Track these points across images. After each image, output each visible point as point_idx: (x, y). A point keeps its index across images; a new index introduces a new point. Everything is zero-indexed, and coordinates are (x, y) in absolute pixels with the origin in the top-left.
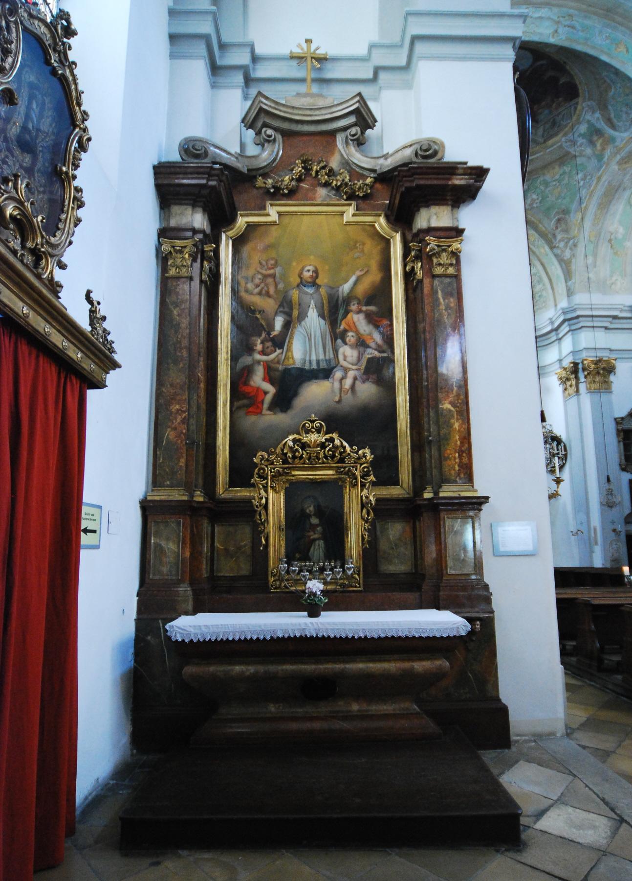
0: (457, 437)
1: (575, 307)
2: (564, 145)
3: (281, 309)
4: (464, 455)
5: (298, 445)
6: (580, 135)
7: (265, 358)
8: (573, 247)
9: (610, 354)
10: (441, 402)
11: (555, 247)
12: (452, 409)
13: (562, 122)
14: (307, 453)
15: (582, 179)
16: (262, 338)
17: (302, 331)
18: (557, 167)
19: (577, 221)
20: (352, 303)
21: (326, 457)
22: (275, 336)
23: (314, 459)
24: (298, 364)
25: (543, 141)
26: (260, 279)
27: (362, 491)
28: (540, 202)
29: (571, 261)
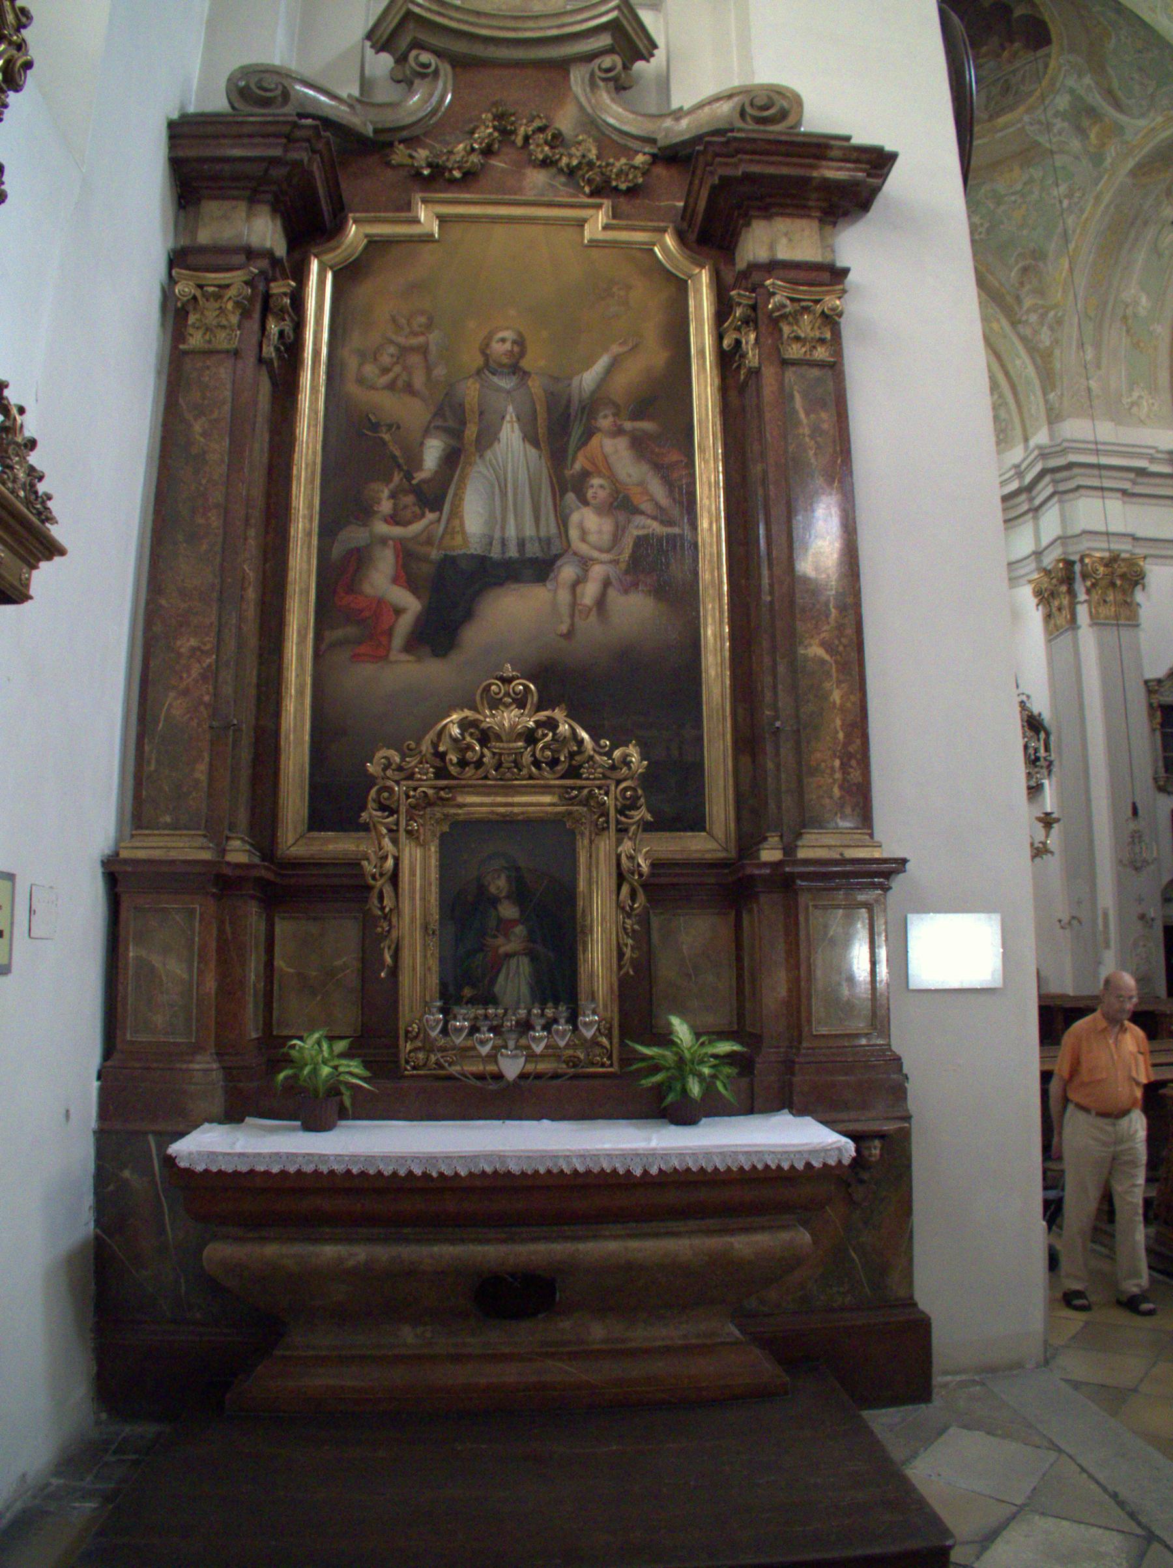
0: (838, 722)
1: (1065, 444)
2: (1027, 127)
3: (439, 423)
4: (853, 763)
5: (471, 735)
6: (1057, 114)
7: (397, 531)
9: (1133, 546)
10: (801, 643)
11: (1020, 322)
12: (827, 657)
13: (1022, 88)
14: (494, 754)
15: (1065, 197)
16: (392, 486)
17: (485, 472)
18: (1017, 169)
20: (602, 414)
21: (536, 763)
22: (423, 481)
23: (509, 768)
24: (475, 548)
26: (392, 356)
27: (619, 842)
28: (988, 232)
29: (1052, 353)
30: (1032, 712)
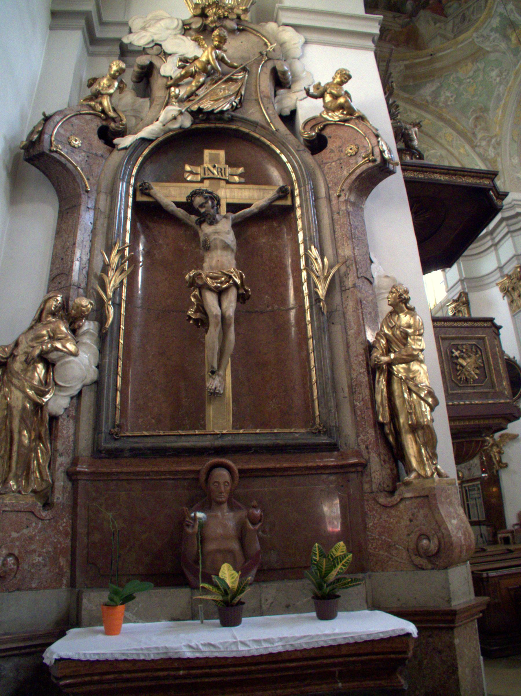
1: (514, 203)
2: (476, 40)
8: (497, 146)
11: (476, 146)
13: (472, 17)
15: (498, 76)
18: (470, 64)
19: (497, 118)
25: (452, 36)
28: (455, 100)
29: (495, 161)
30: (509, 357)
